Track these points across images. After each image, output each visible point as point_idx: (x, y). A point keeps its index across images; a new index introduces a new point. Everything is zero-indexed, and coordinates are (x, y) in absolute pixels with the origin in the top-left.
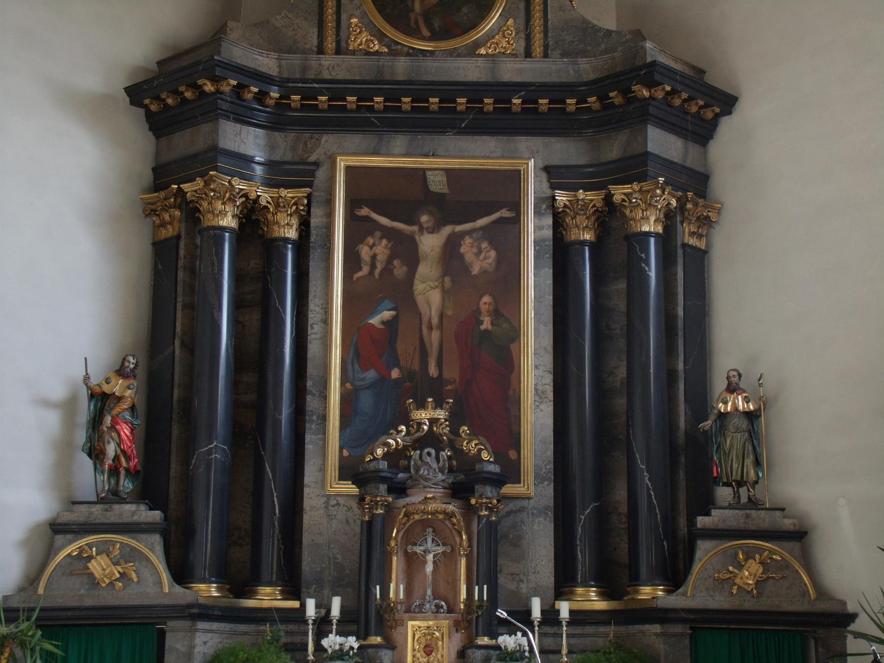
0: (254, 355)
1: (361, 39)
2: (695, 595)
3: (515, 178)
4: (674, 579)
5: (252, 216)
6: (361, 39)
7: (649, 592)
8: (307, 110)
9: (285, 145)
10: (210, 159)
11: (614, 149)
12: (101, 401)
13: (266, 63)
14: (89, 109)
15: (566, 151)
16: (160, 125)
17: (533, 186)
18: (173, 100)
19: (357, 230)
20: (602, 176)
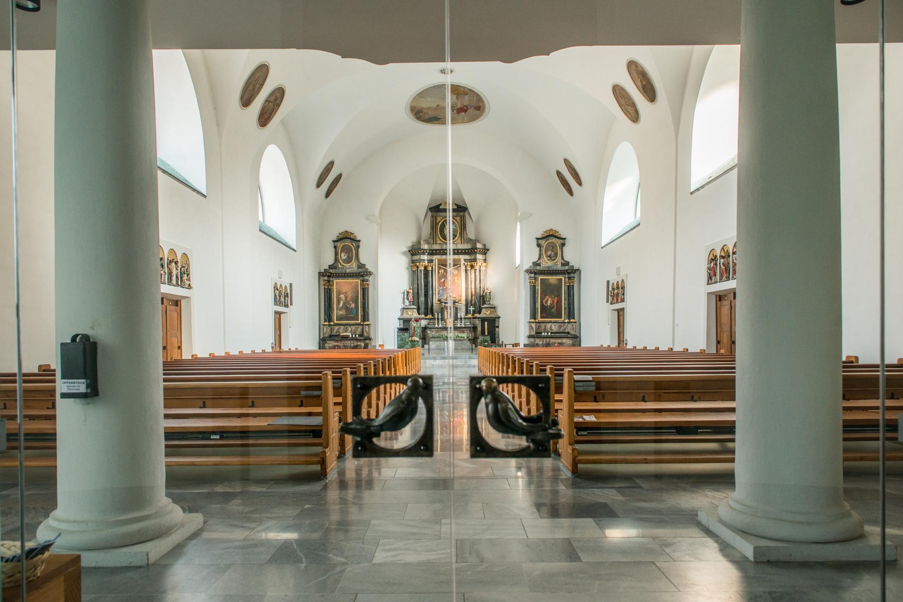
0: (426, 286)
1: (439, 242)
2: (482, 315)
3: (460, 260)
4: (480, 313)
5: (426, 268)
6: (439, 242)
7: (477, 315)
8: (432, 252)
9: (430, 257)
10: (420, 261)
11: (473, 257)
12: (408, 292)
13: (426, 247)
14: (404, 253)
15: (467, 257)
16: (413, 255)
17: (462, 262)
18: (414, 251)
19: (439, 268)
20: (471, 261)
